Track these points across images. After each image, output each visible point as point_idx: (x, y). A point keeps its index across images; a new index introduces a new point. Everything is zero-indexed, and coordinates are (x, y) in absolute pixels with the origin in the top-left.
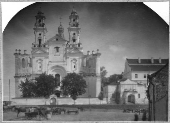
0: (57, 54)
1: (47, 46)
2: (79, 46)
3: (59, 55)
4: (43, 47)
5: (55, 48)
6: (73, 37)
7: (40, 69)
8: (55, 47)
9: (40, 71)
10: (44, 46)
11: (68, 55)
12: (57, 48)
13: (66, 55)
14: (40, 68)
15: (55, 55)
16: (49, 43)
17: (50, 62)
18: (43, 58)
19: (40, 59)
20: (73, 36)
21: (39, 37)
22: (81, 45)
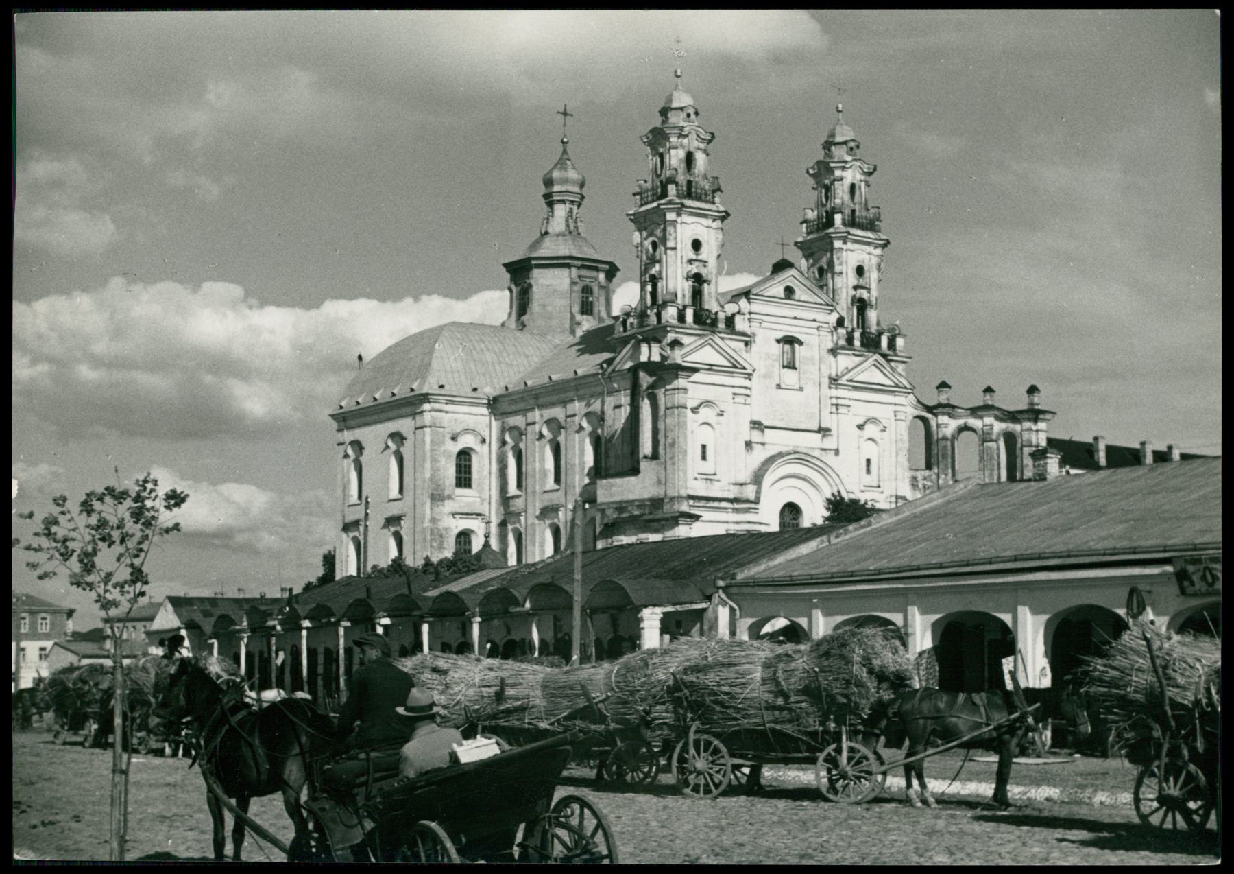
0: (790, 377)
1: (740, 324)
2: (892, 344)
3: (801, 389)
4: (722, 326)
5: (778, 341)
6: (856, 288)
7: (707, 467)
8: (780, 335)
9: (709, 478)
10: (730, 321)
11: (842, 393)
12: (787, 347)
13: (834, 392)
14: (704, 458)
15: (779, 386)
16: (756, 307)
17: (757, 425)
18: (723, 396)
19: (708, 403)
20: (855, 283)
21: (690, 262)
22: (900, 342)
